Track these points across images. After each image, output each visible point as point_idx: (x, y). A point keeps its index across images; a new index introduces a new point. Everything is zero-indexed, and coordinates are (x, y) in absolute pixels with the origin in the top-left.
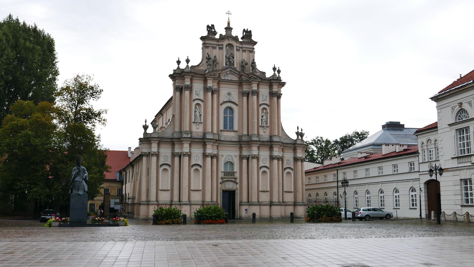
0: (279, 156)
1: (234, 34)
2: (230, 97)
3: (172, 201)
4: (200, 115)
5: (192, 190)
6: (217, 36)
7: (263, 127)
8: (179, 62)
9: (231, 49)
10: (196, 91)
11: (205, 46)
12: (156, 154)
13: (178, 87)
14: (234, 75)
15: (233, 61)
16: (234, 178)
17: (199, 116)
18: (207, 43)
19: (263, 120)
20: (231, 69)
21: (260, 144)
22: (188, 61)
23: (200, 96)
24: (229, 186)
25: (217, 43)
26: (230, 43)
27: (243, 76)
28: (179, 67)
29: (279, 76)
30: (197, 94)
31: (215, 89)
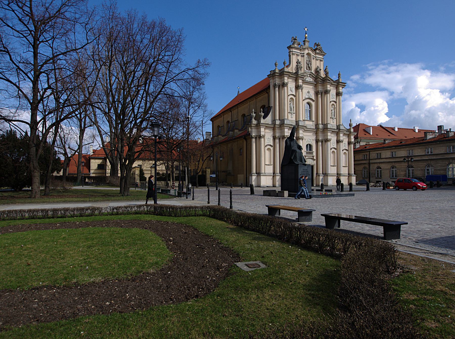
4: (294, 107)
14: (311, 77)
26: (309, 53)
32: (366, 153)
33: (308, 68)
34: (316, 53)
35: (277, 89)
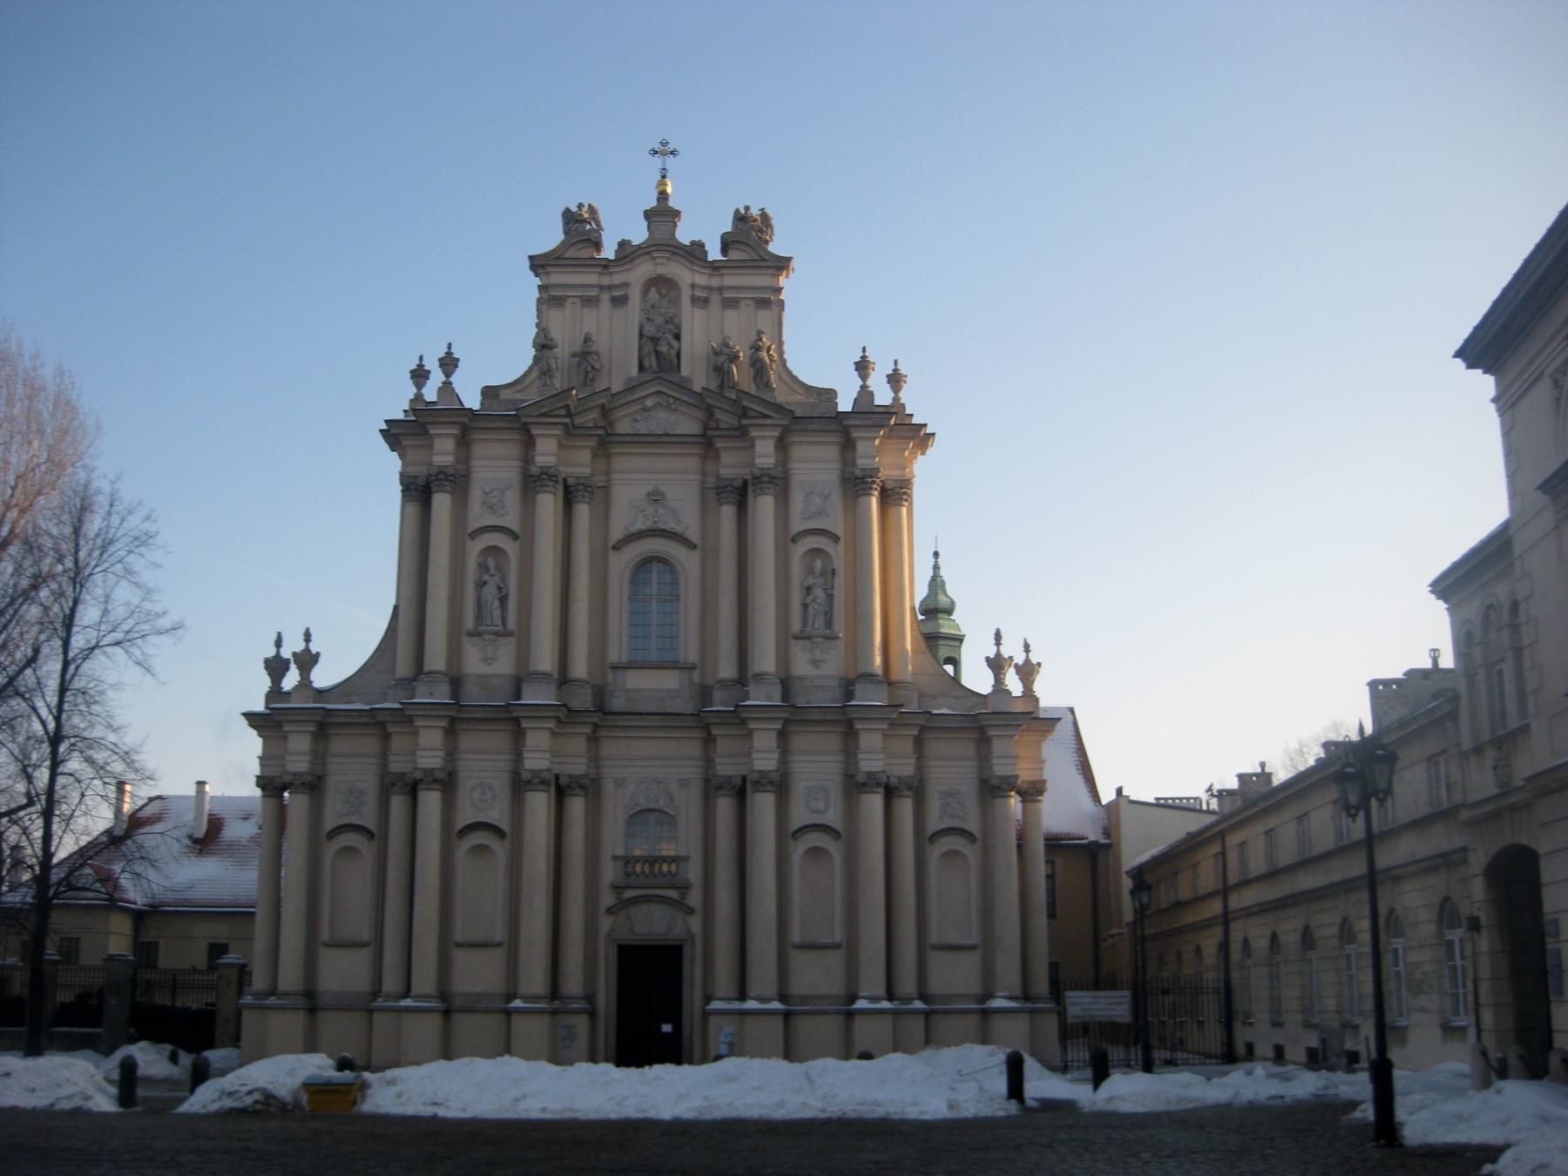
0: (884, 772)
1: (684, 235)
3: (376, 993)
4: (503, 601)
5: (459, 945)
6: (609, 252)
7: (809, 638)
8: (419, 375)
9: (670, 300)
10: (486, 493)
11: (549, 299)
12: (303, 784)
13: (411, 483)
14: (676, 410)
15: (674, 353)
16: (674, 887)
17: (496, 603)
19: (811, 610)
20: (660, 384)
21: (786, 722)
22: (449, 363)
23: (502, 515)
24: (652, 924)
25: (605, 281)
28: (422, 396)
29: (896, 399)
30: (491, 507)
31: (582, 481)
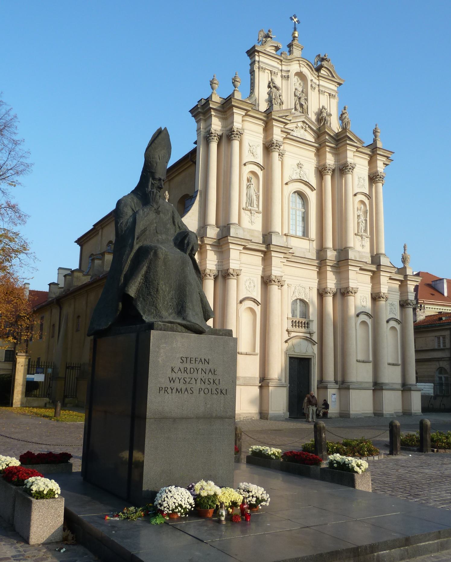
2: (301, 172)
10: (250, 146)
14: (306, 130)
16: (310, 333)
18: (262, 62)
27: (326, 134)
32: (443, 333)
33: (298, 107)
34: (318, 76)
35: (214, 146)
